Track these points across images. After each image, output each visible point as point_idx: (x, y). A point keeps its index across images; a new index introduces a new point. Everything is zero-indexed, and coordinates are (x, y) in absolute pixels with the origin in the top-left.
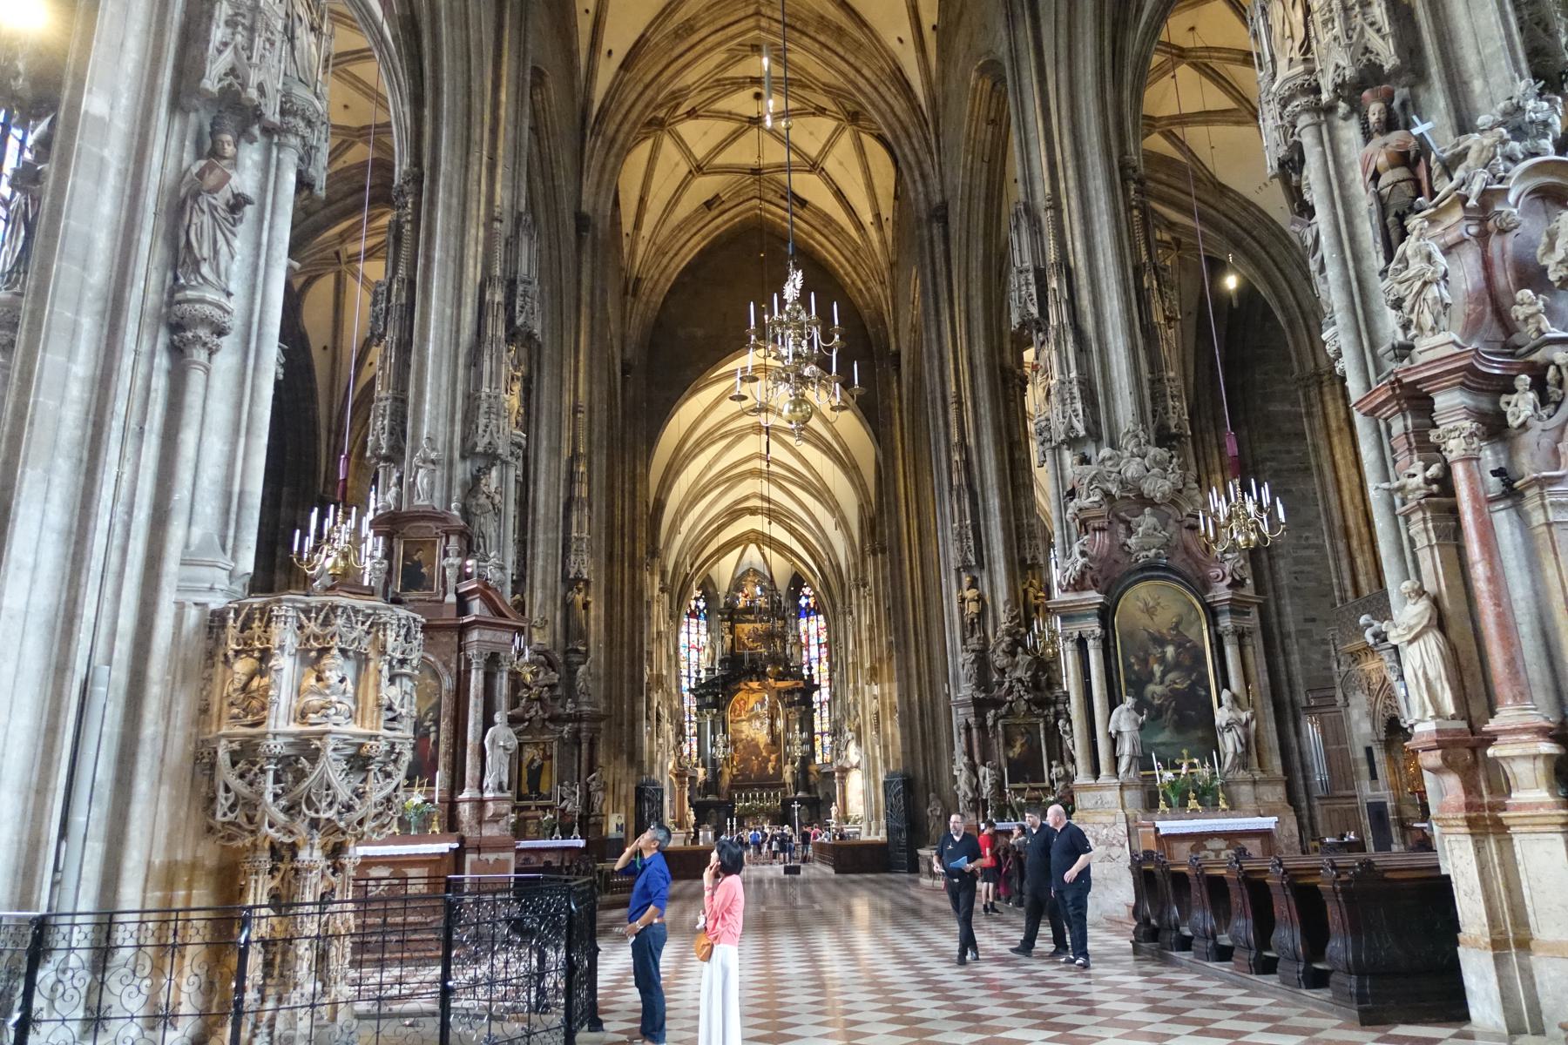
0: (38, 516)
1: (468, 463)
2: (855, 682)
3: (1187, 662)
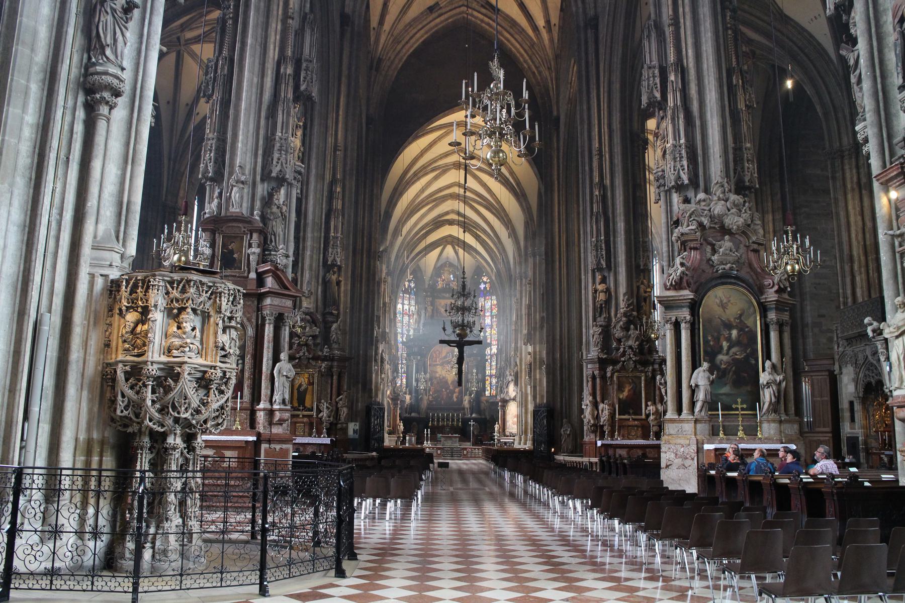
0: (5, 215)
1: (266, 185)
2: (516, 343)
3: (745, 341)
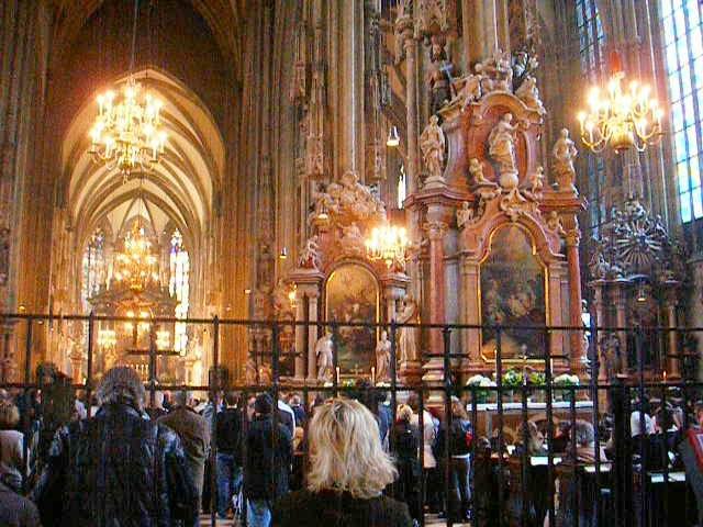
2: (201, 304)
3: (365, 311)
